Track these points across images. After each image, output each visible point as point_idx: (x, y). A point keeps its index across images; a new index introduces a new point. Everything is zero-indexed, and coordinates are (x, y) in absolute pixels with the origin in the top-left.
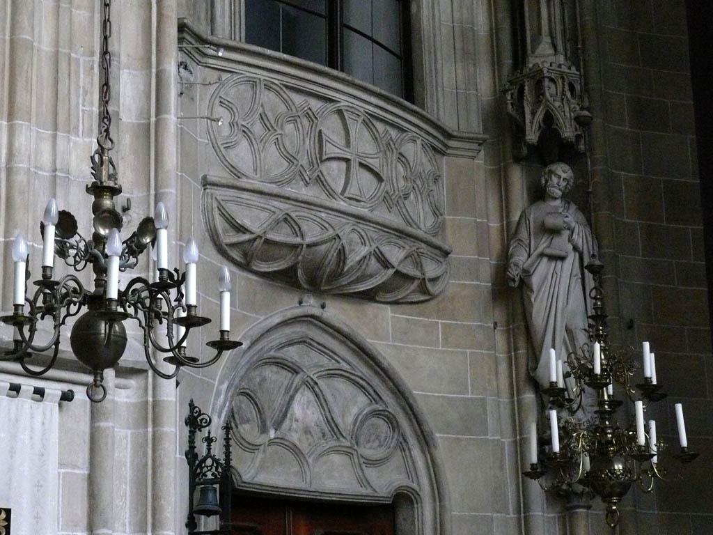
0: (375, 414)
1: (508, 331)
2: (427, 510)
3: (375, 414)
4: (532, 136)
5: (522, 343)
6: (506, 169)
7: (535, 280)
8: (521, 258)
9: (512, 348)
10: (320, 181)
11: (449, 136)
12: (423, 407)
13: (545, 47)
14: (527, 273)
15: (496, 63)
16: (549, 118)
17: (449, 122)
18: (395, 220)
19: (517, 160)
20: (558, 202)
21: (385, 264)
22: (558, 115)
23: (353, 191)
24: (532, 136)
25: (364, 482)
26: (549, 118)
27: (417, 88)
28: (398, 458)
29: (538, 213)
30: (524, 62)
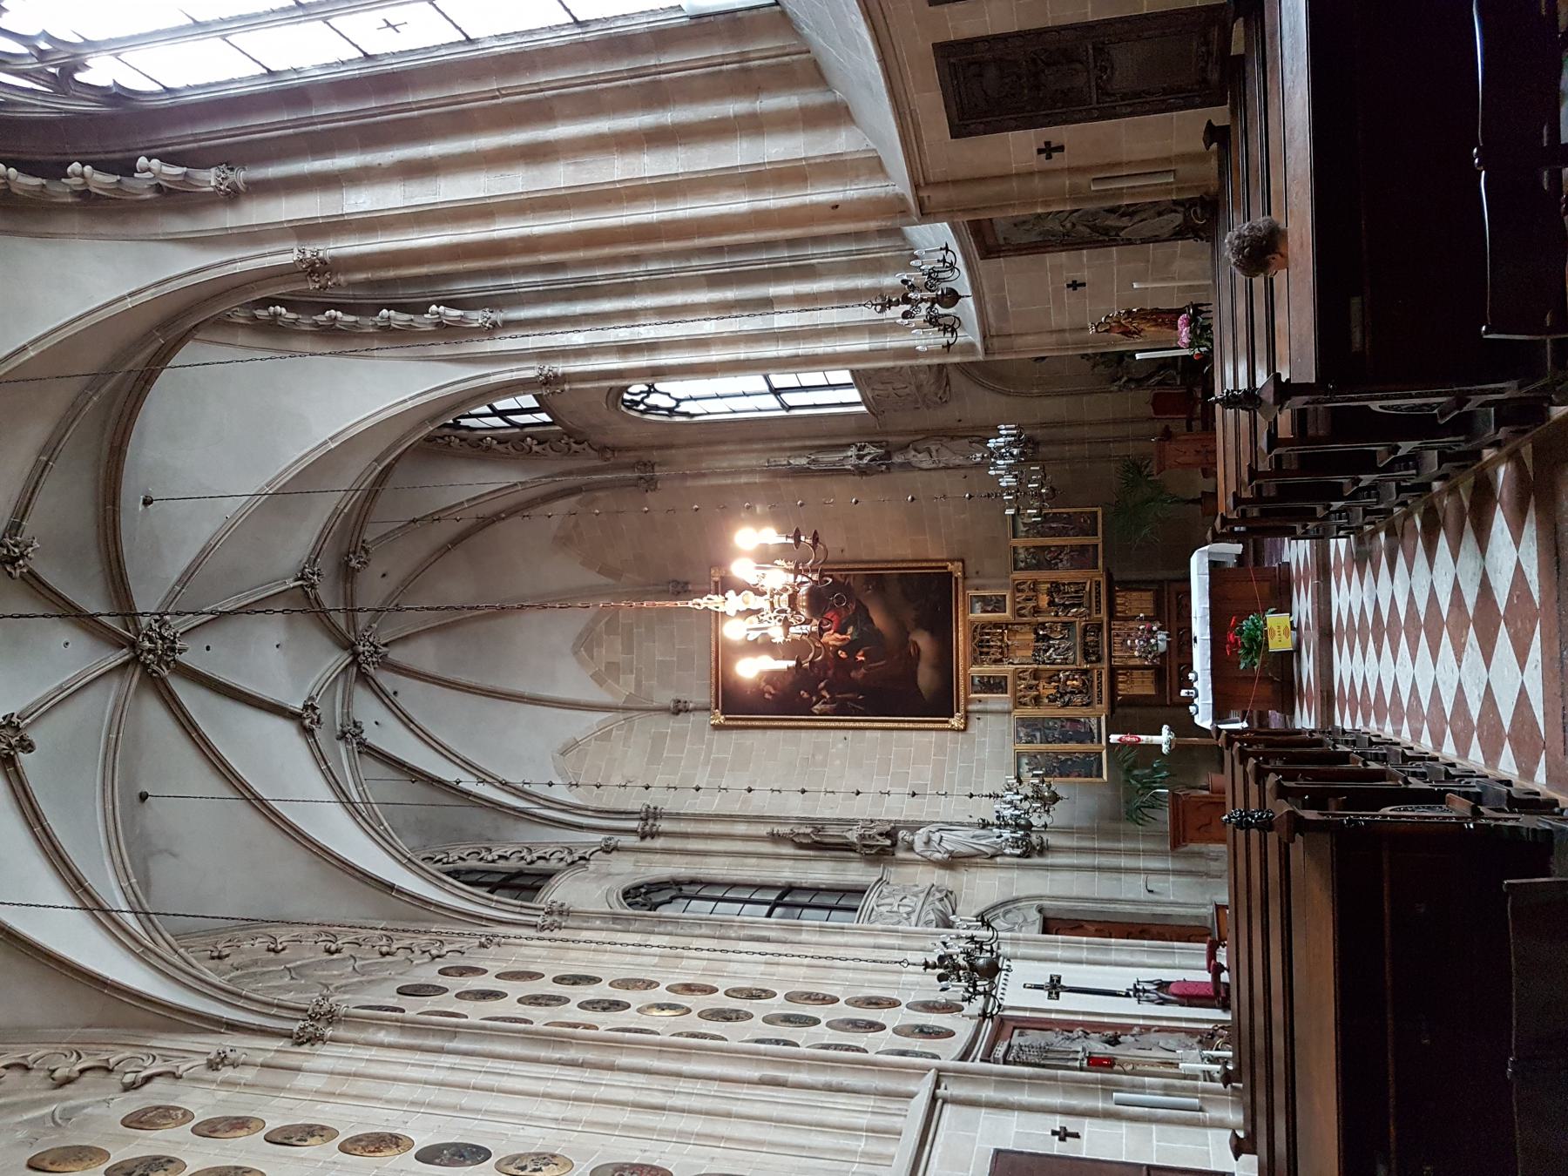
0: (1004, 916)
1: (970, 867)
2: (1046, 903)
3: (1004, 916)
4: (888, 842)
5: (974, 860)
6: (897, 860)
7: (950, 848)
8: (938, 856)
9: (976, 865)
10: (908, 914)
11: (881, 879)
12: (1001, 899)
13: (848, 834)
14: (947, 851)
15: (849, 860)
16: (881, 834)
17: (876, 879)
18: (922, 896)
19: (893, 855)
20: (916, 837)
21: (941, 900)
22: (879, 831)
23: (913, 904)
24: (888, 842)
25: (1034, 923)
26: (881, 834)
27: (860, 888)
28: (1025, 912)
29: (919, 846)
30: (854, 844)
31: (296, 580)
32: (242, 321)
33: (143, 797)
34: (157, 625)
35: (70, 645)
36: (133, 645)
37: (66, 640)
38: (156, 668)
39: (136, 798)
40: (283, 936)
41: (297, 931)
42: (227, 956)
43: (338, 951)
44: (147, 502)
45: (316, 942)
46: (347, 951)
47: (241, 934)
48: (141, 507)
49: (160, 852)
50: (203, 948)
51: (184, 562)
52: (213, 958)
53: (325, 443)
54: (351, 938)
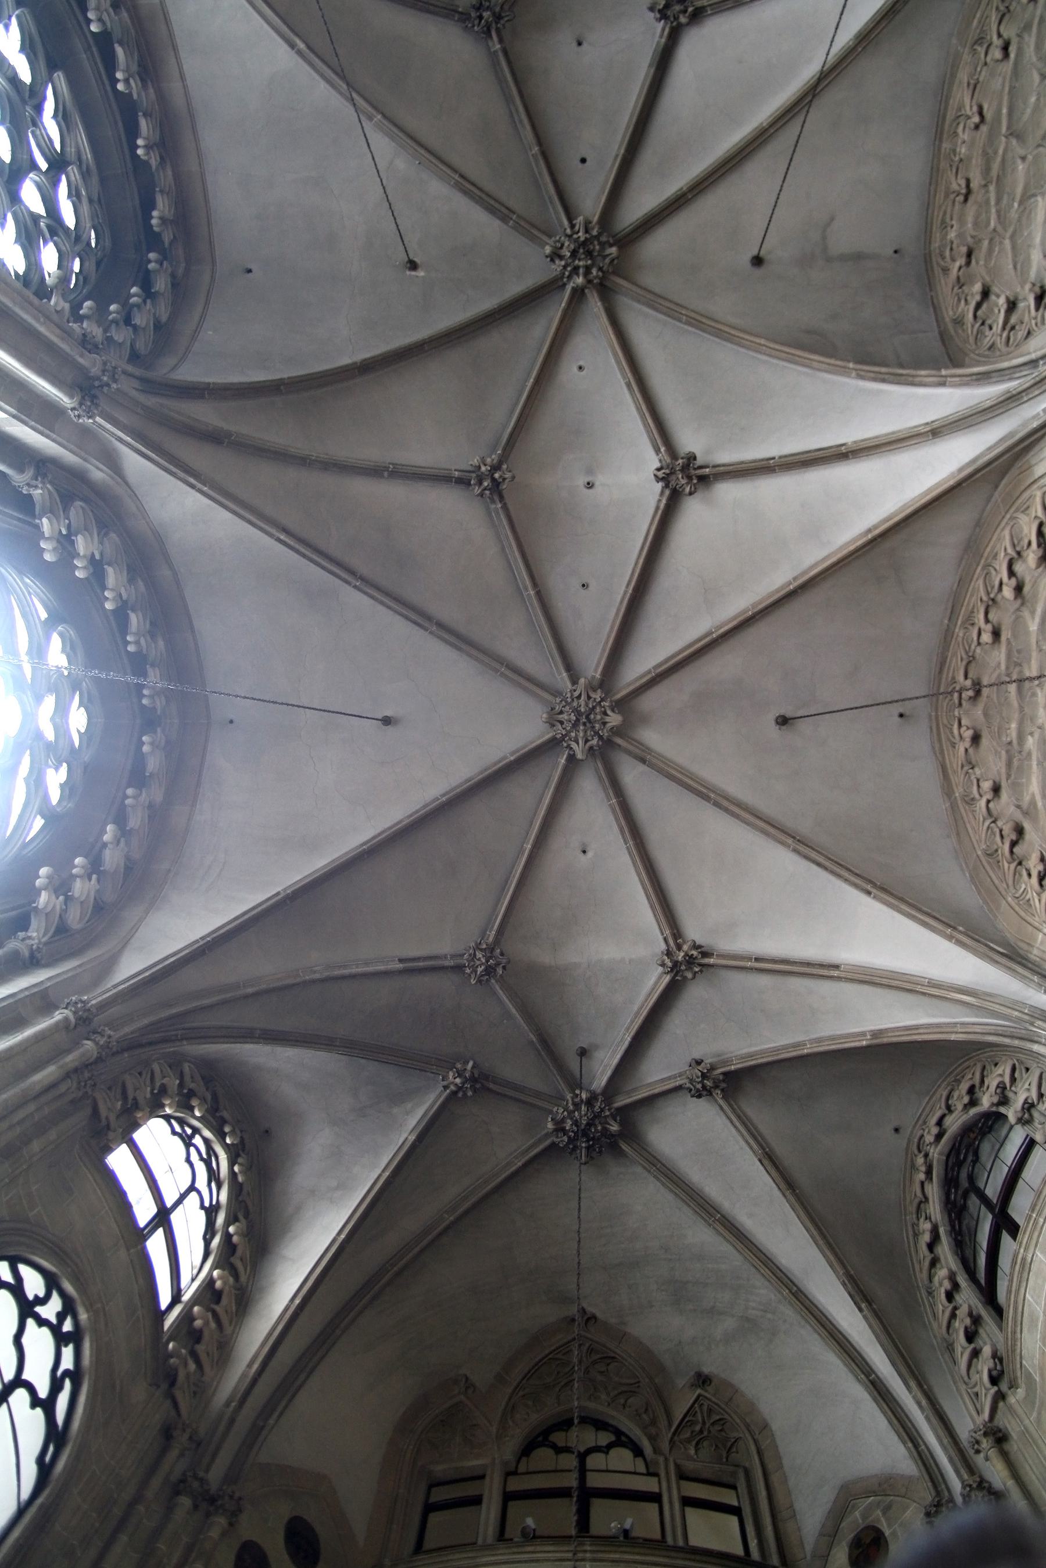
31: (491, 37)
32: (169, 173)
33: (758, 261)
34: (557, 261)
35: (581, 363)
36: (578, 294)
37: (575, 369)
38: (607, 261)
39: (758, 272)
40: (963, 98)
41: (963, 76)
42: (968, 182)
43: (1006, 48)
44: (413, 265)
45: (986, 64)
46: (1009, 31)
47: (946, 145)
48: (421, 273)
49: (824, 238)
50: (950, 203)
51: (479, 216)
52: (966, 200)
53: (299, 53)
54: (994, 18)
